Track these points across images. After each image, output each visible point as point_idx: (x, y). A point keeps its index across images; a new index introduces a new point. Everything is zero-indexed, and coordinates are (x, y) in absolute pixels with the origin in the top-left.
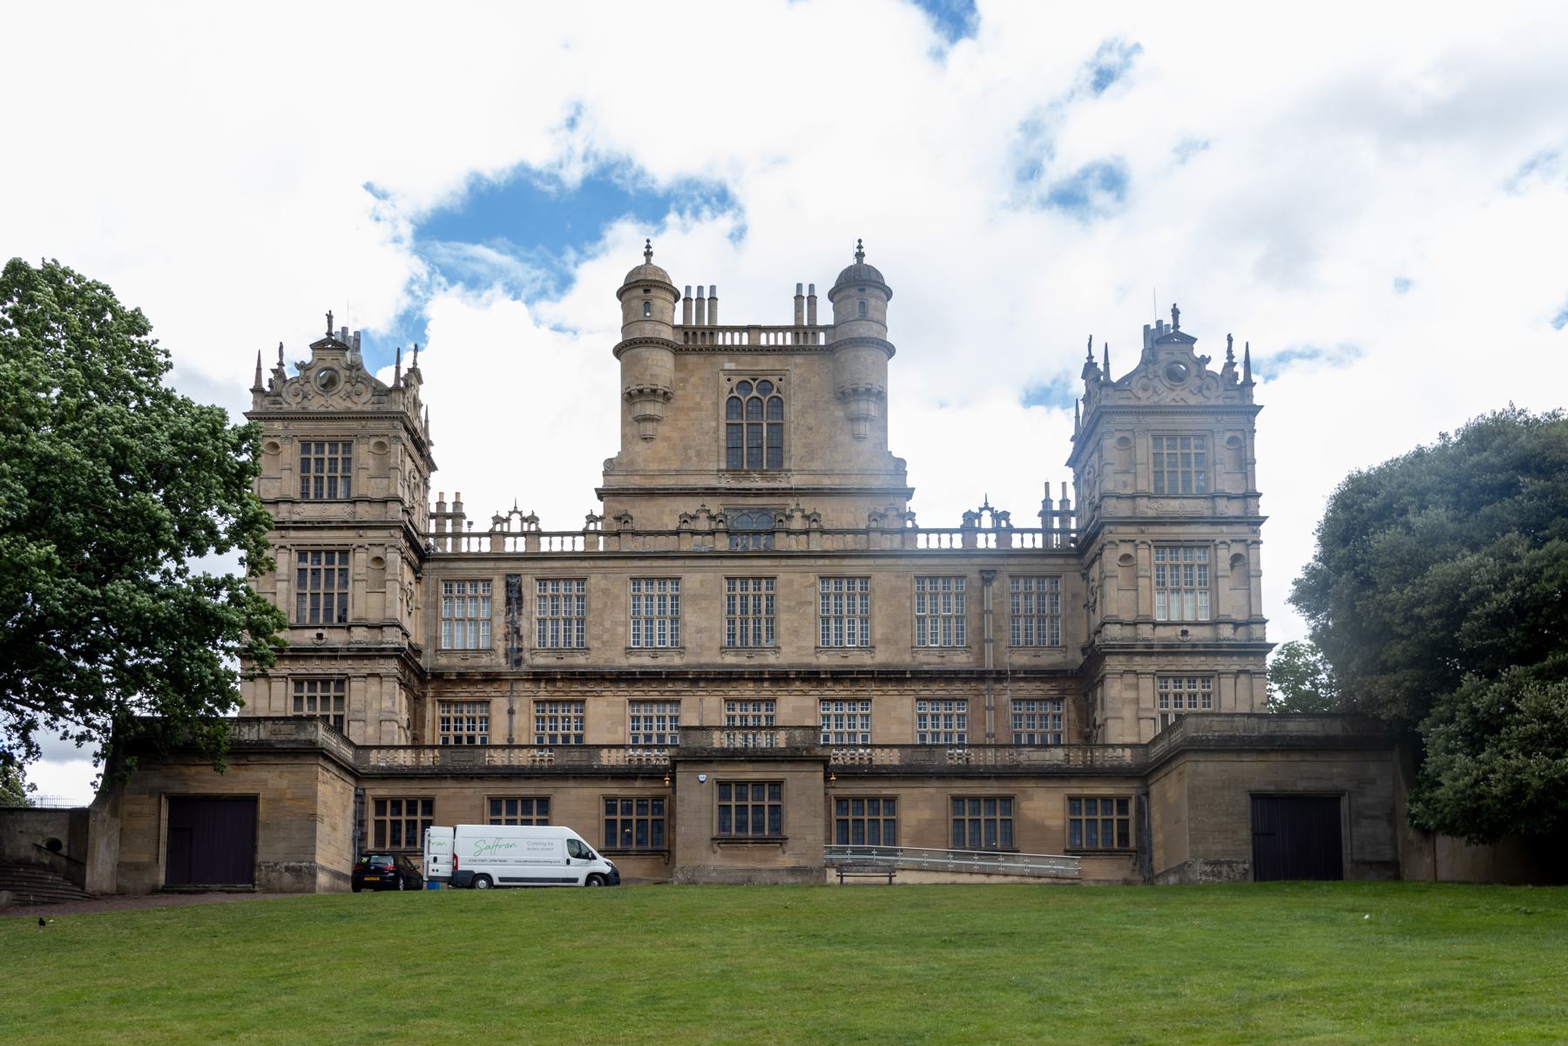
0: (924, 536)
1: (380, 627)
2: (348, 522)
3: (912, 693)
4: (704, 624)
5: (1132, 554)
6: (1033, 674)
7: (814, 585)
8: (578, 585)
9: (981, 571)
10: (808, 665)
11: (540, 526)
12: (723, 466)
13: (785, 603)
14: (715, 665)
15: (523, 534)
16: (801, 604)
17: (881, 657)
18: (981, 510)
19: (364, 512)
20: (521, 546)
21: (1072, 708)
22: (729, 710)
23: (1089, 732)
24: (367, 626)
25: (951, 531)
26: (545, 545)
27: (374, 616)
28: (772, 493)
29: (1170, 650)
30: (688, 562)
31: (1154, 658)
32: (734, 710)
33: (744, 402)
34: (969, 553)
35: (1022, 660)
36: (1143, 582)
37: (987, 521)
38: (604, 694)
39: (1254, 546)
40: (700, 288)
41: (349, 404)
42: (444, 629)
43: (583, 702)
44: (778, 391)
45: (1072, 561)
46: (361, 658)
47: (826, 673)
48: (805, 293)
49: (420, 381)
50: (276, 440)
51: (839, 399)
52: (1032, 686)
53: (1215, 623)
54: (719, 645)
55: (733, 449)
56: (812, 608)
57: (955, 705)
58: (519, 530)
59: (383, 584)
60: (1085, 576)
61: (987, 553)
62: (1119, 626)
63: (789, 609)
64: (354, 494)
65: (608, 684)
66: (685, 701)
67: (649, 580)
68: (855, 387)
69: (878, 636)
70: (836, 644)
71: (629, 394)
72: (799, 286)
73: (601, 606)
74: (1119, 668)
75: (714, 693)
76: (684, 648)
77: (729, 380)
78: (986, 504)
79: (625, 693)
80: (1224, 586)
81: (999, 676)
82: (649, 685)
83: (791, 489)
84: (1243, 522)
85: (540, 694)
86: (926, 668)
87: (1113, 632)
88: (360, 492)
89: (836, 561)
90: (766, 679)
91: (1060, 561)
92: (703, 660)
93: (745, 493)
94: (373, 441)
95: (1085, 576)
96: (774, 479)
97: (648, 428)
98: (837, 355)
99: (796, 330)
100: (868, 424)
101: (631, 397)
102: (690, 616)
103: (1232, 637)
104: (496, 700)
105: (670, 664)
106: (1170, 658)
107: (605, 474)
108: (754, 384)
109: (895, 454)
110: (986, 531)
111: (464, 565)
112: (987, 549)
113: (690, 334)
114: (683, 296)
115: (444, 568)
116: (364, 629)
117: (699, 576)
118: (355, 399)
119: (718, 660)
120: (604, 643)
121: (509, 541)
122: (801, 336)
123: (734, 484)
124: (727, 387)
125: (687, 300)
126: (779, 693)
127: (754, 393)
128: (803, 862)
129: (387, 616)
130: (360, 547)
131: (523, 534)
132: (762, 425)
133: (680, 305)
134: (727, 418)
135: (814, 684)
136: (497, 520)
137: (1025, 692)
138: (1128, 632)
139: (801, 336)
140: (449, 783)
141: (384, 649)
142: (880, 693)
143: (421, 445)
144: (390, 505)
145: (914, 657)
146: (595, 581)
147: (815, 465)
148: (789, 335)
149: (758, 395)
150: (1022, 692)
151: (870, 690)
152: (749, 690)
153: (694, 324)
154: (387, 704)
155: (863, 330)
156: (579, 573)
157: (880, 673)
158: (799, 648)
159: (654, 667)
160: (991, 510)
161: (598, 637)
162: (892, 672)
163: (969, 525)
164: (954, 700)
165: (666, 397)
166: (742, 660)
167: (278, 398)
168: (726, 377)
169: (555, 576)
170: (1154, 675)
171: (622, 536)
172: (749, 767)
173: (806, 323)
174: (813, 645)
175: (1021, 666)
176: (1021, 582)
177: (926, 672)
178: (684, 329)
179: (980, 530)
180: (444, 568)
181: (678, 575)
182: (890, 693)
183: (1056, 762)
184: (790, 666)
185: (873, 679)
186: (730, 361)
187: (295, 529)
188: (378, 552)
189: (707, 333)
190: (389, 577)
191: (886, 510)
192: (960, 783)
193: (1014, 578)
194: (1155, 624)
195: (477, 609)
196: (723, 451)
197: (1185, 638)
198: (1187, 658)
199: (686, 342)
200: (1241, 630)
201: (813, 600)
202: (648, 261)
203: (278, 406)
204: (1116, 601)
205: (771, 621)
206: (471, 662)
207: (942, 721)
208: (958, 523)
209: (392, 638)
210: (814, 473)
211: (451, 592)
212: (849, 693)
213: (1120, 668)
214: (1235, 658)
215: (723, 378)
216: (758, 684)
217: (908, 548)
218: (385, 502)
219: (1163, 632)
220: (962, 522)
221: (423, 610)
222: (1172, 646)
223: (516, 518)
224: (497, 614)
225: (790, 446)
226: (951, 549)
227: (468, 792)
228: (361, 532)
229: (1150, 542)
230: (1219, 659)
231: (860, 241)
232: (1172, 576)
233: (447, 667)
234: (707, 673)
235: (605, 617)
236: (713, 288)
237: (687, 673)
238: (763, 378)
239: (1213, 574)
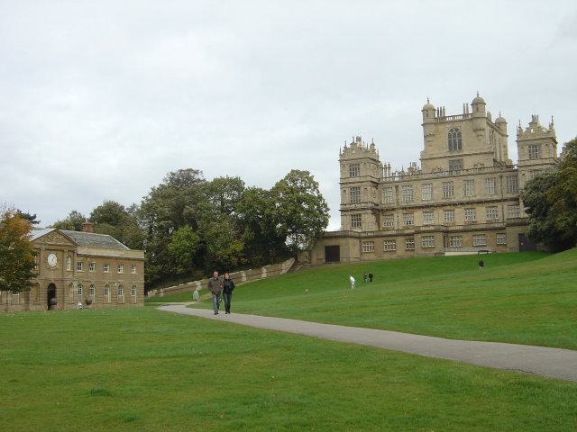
6: (511, 199)
17: (478, 198)
27: (365, 201)
35: (510, 196)
55: (450, 145)
81: (505, 200)
102: (435, 192)
151: (475, 206)
152: (448, 208)
155: (477, 115)
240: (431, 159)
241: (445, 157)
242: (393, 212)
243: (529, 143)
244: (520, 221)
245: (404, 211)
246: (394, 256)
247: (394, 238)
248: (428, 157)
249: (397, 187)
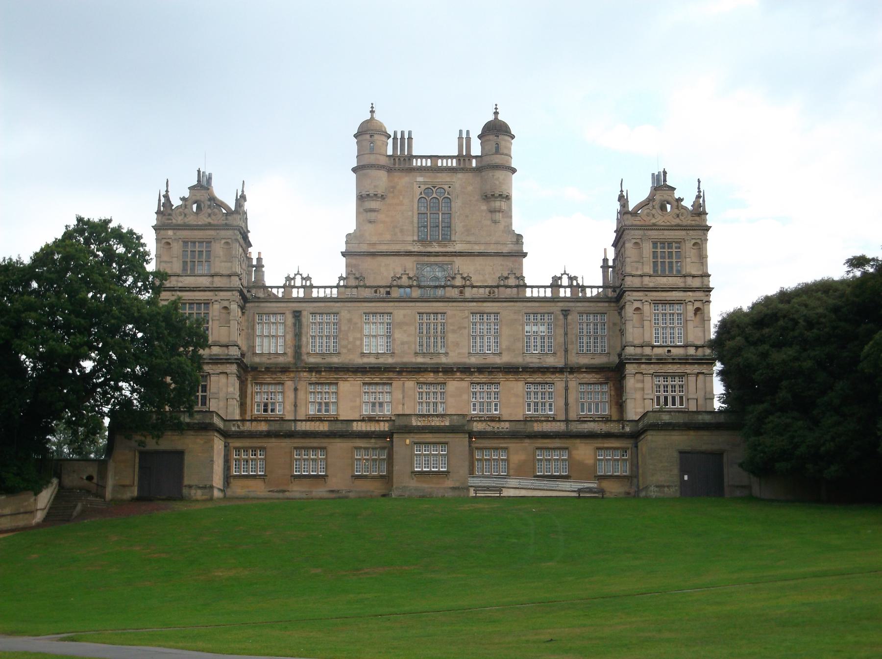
0: (530, 289)
1: (227, 346)
2: (209, 287)
3: (523, 379)
5: (641, 307)
7: (467, 317)
8: (334, 316)
9: (562, 310)
10: (465, 364)
11: (312, 282)
12: (416, 238)
13: (451, 328)
14: (412, 363)
15: (302, 287)
16: (461, 328)
17: (505, 359)
18: (562, 274)
19: (218, 282)
20: (301, 293)
21: (612, 388)
22: (419, 388)
23: (620, 404)
24: (220, 346)
25: (545, 287)
26: (315, 293)
27: (224, 340)
28: (445, 254)
29: (661, 361)
30: (396, 304)
31: (652, 366)
32: (422, 388)
33: (429, 200)
34: (555, 299)
35: (584, 361)
36: (646, 323)
37: (565, 281)
38: (348, 379)
39: (707, 303)
40: (402, 133)
41: (209, 220)
42: (258, 341)
43: (337, 384)
45: (613, 304)
46: (217, 363)
47: (474, 368)
48: (464, 136)
49: (245, 200)
50: (168, 241)
51: (484, 199)
52: (590, 376)
53: (685, 346)
54: (414, 352)
56: (467, 331)
57: (547, 386)
58: (300, 285)
59: (228, 322)
60: (620, 314)
61: (565, 299)
62: (633, 347)
63: (454, 331)
64: (213, 272)
65: (351, 374)
66: (395, 384)
67: (374, 314)
69: (504, 347)
70: (480, 351)
71: (361, 196)
72: (461, 131)
73: (346, 328)
74: (633, 371)
75: (411, 379)
77: (419, 187)
78: (565, 271)
79: (361, 379)
80: (690, 325)
82: (374, 375)
83: (456, 252)
84: (701, 291)
85: (312, 379)
86: (531, 365)
87: (630, 350)
88: (216, 270)
89: (480, 304)
91: (606, 304)
93: (429, 254)
94: (223, 241)
95: (620, 314)
96: (446, 246)
97: (372, 215)
98: (483, 173)
99: (459, 157)
100: (501, 214)
101: (361, 198)
102: (398, 335)
103: (695, 354)
104: (288, 382)
105: (386, 362)
106: (661, 366)
107: (347, 243)
108: (434, 190)
109: (517, 232)
110: (565, 287)
111: (269, 304)
112: (565, 297)
113: (397, 159)
114: (392, 137)
115: (258, 306)
116: (218, 347)
117: (402, 312)
118: (213, 217)
119: (414, 360)
120: (349, 350)
121: (295, 291)
122: (462, 161)
123: (422, 249)
124: (418, 191)
125: (395, 139)
126: (447, 379)
127: (434, 195)
128: (457, 485)
129: (231, 339)
130: (216, 301)
131: (302, 287)
132: (439, 214)
133: (390, 141)
134: (418, 210)
135: (468, 374)
136: (288, 279)
137: (586, 379)
138: (638, 351)
139: (462, 161)
140: (273, 440)
141: (229, 359)
142: (504, 379)
143: (245, 238)
144: (232, 277)
145: (524, 359)
146: (345, 314)
147: (471, 238)
148: (454, 161)
150: (584, 379)
152: (430, 377)
153: (399, 154)
154: (231, 389)
155: (498, 159)
156: (334, 310)
157: (504, 368)
158: (459, 353)
159: (376, 364)
160: (568, 275)
161: (345, 347)
162: (512, 368)
163: (555, 284)
164: (547, 383)
165: (383, 197)
166: (427, 360)
167: (170, 217)
169: (320, 312)
170: (652, 375)
171: (359, 288)
172: (430, 435)
173: (464, 154)
174: (467, 352)
175: (584, 364)
176: (585, 316)
177: (531, 368)
178: (393, 157)
179: (561, 286)
180: (258, 306)
181: (391, 311)
182: (511, 379)
183: (590, 430)
184: (455, 364)
185: (501, 371)
187: (180, 291)
188: (226, 304)
189: (407, 159)
190: (233, 318)
191: (509, 274)
192: (540, 441)
193: (581, 314)
194: (653, 347)
195: (277, 329)
196: (416, 230)
197: (669, 354)
198: (670, 366)
199: (394, 164)
200: (700, 349)
201: (467, 327)
202: (372, 116)
203: (170, 221)
204: (633, 334)
205: (443, 338)
206: (273, 361)
207: (540, 396)
208: (549, 282)
209: (234, 352)
210: (469, 242)
211: (261, 320)
212: (487, 379)
213: (634, 371)
214: (696, 366)
215: (416, 186)
216: (436, 374)
217: (520, 296)
218: (229, 276)
219: (657, 351)
220: (551, 282)
221: (246, 331)
222: (661, 359)
223: (298, 278)
224: (288, 333)
225: (455, 227)
226: (545, 297)
227: (283, 445)
228: (217, 293)
229: (650, 301)
230: (687, 366)
231: (496, 105)
232: (663, 319)
233: (260, 364)
234: (407, 368)
235: (349, 335)
236: (410, 133)
239: (685, 319)
240: (373, 254)
241: (409, 254)
242: (284, 377)
243: (654, 234)
244: (680, 419)
245: (314, 377)
246: (320, 491)
247: (324, 442)
248: (364, 248)
249: (297, 315)
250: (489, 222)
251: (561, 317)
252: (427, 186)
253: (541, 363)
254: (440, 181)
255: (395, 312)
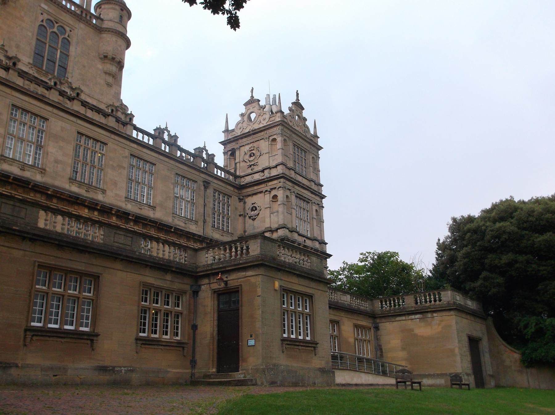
4: (60, 158)
9: (204, 182)
30: (55, 111)
44: (68, 36)
45: (236, 191)
51: (101, 59)
54: (69, 176)
68: (114, 56)
76: (45, 170)
89: (140, 148)
90: (97, 210)
91: (232, 189)
92: (58, 183)
102: (52, 149)
108: (56, 25)
127: (55, 30)
135: (123, 221)
145: (173, 220)
149: (57, 32)
158: (116, 195)
168: (41, 12)
171: (11, 71)
181: (47, 117)
185: (154, 227)
186: (45, 4)
237: (48, 189)
238: (60, 24)
250: (102, 82)
251: (202, 188)
252: (50, 18)
253: (186, 228)
254: (63, 19)
255: (52, 120)
